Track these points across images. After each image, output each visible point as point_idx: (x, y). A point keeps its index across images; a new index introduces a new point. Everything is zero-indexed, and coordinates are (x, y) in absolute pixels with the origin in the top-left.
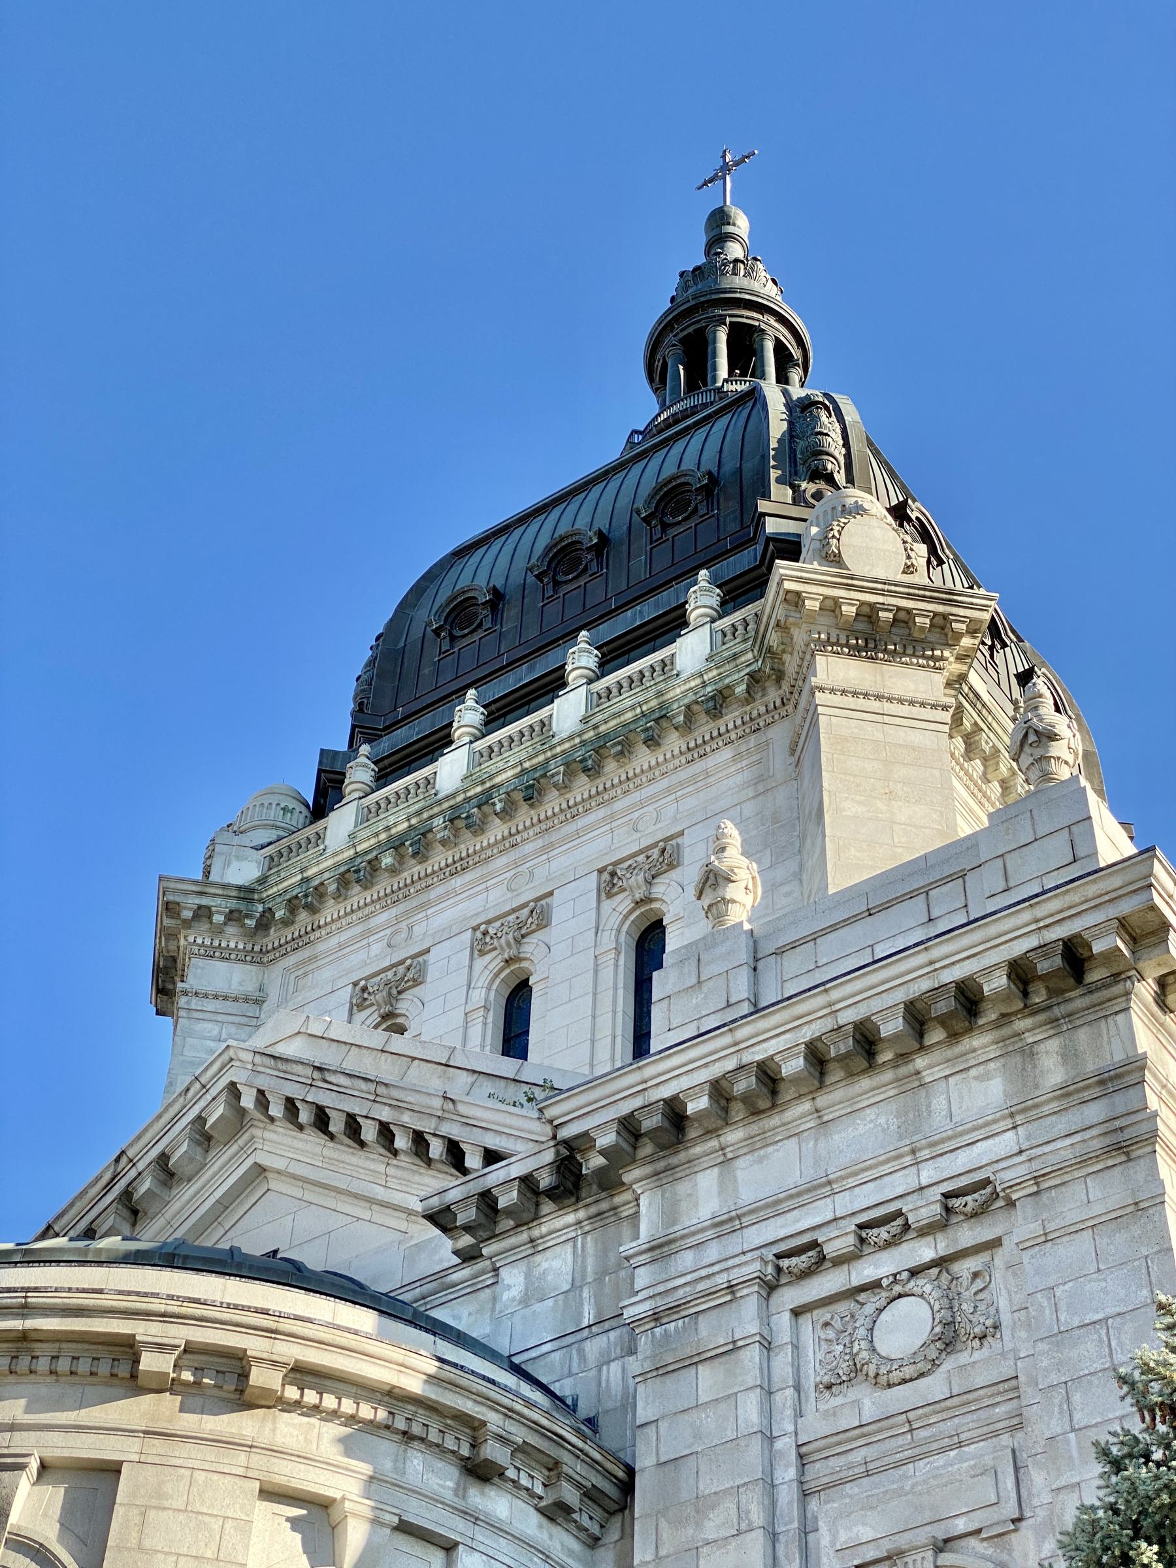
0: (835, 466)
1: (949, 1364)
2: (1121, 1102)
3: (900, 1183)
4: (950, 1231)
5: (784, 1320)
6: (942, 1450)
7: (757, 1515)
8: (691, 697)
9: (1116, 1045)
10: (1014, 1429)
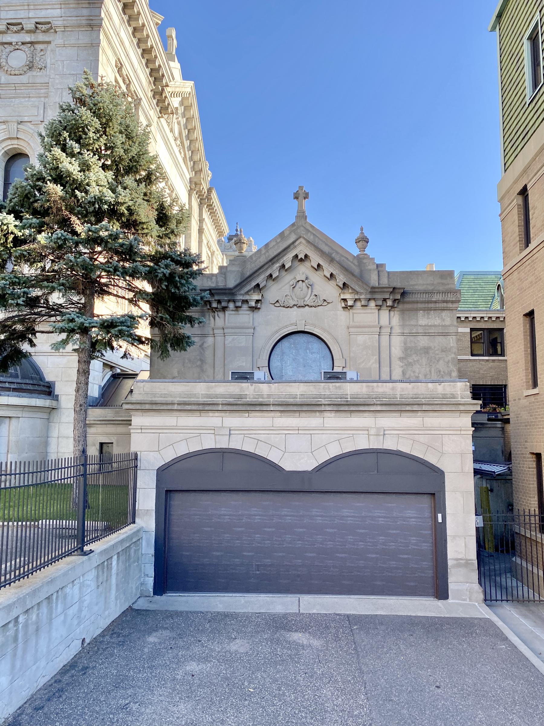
1: (30, 74)
6: (24, 97)
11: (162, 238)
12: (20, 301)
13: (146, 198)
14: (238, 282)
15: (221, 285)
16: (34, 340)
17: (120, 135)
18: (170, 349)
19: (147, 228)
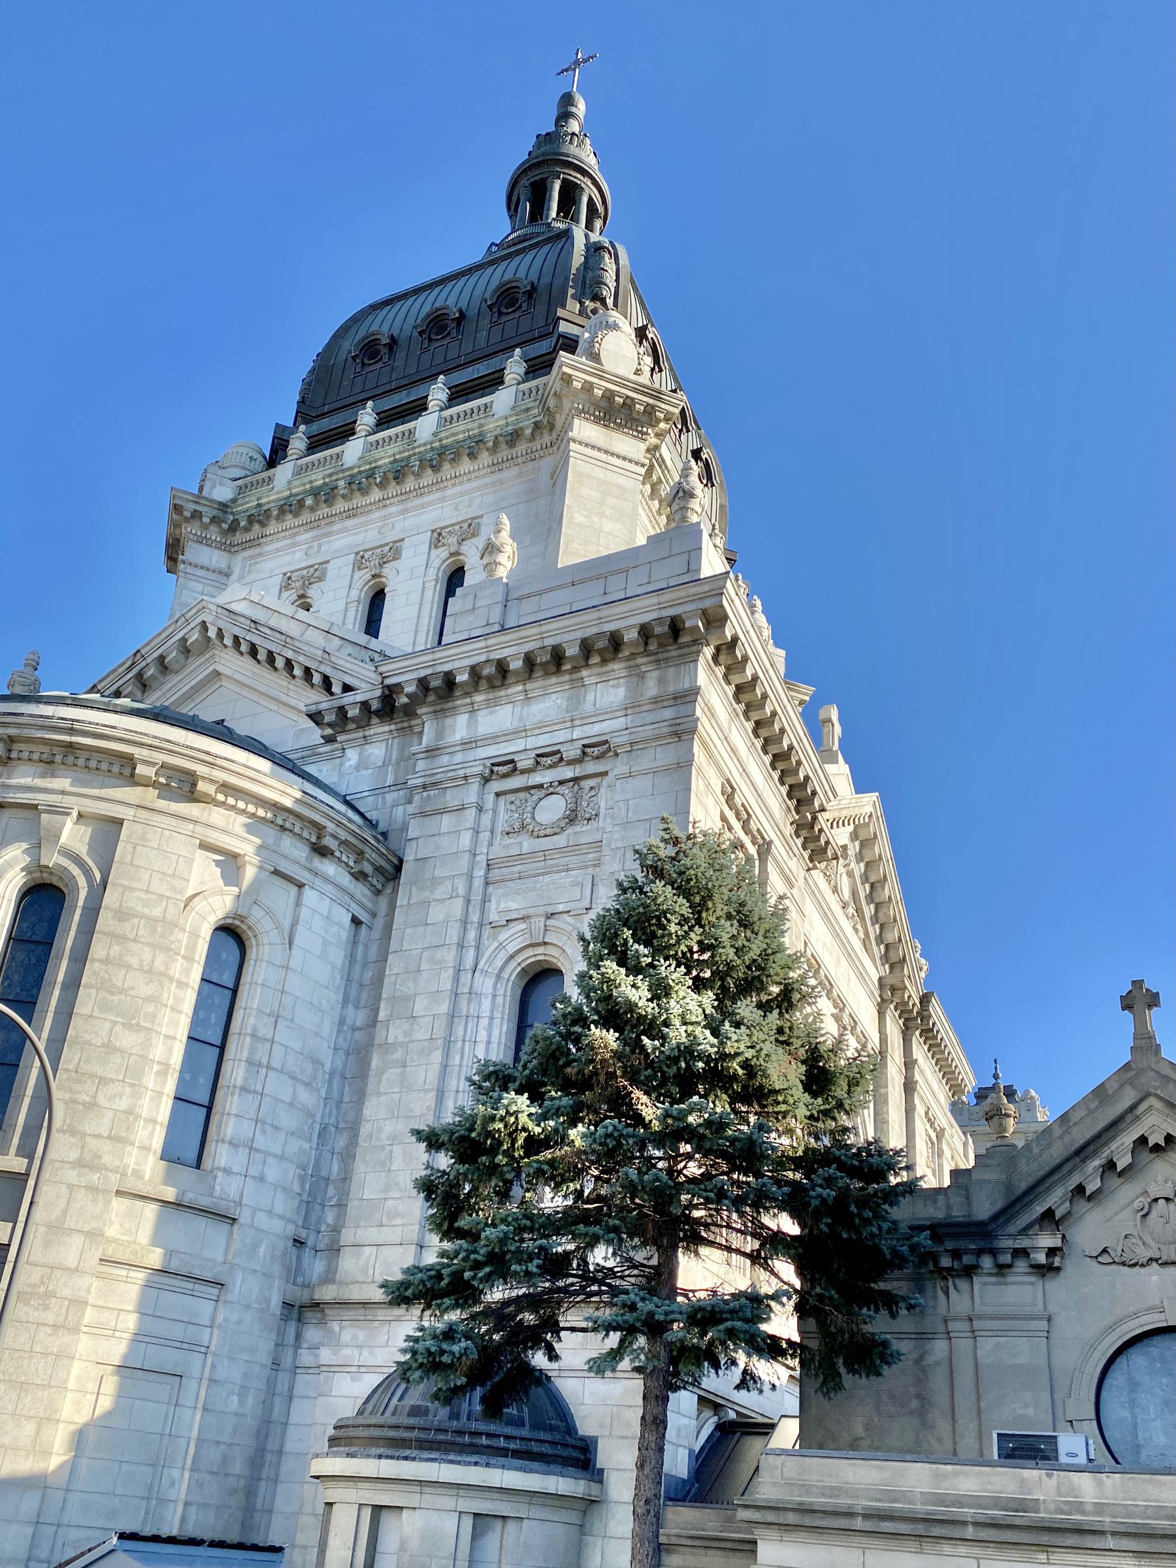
0: (608, 294)
1: (570, 830)
2: (683, 710)
3: (561, 736)
4: (583, 765)
5: (492, 797)
7: (461, 891)
8: (498, 432)
9: (687, 677)
10: (595, 866)
11: (817, 1120)
12: (532, 1267)
13: (781, 1039)
14: (1000, 1204)
15: (958, 1213)
16: (556, 1345)
17: (729, 923)
18: (842, 1370)
19: (785, 1102)
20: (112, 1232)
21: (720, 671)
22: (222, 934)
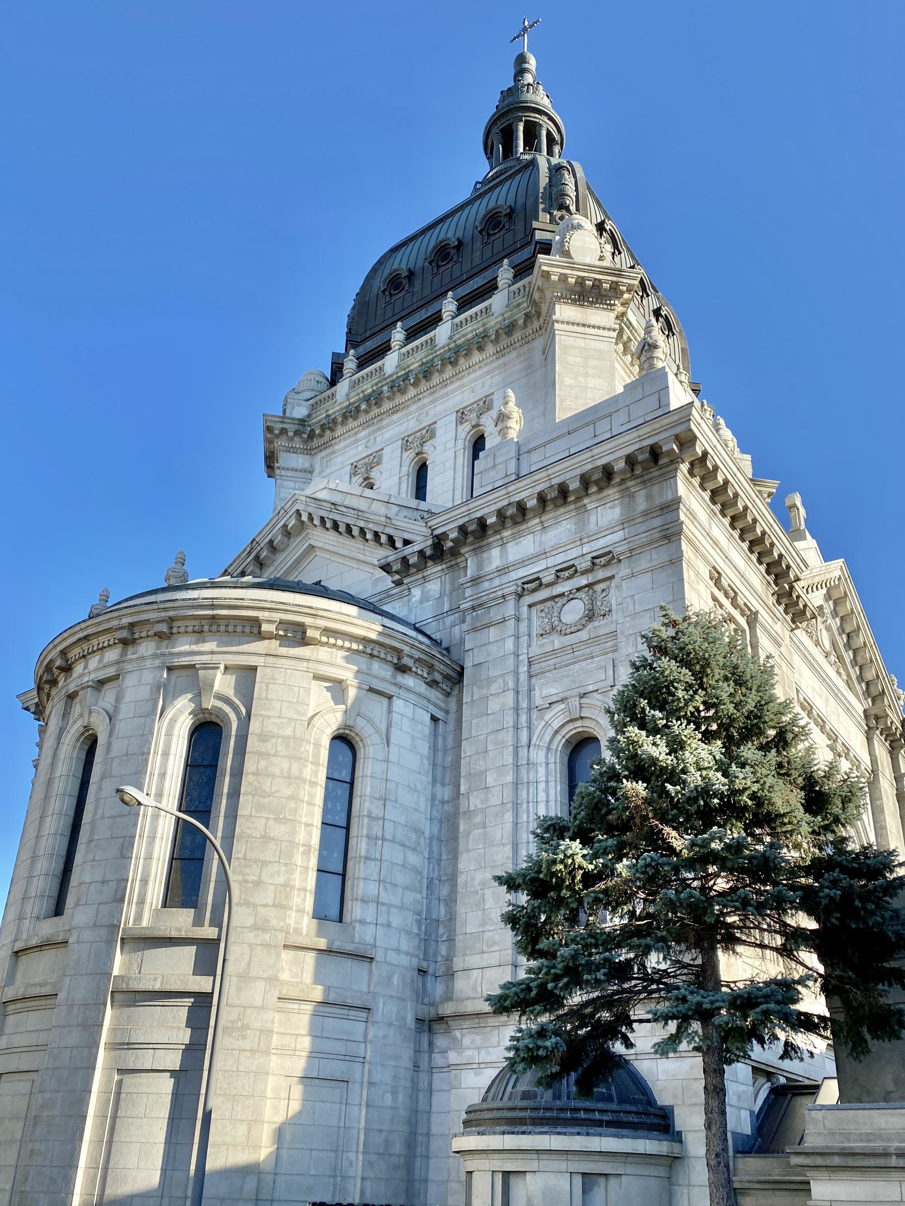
0: (570, 202)
1: (590, 626)
2: (669, 517)
3: (574, 553)
4: (594, 573)
5: (525, 609)
6: (585, 660)
7: (511, 685)
8: (498, 326)
9: (669, 491)
10: (614, 651)
11: (819, 834)
12: (600, 976)
13: (782, 772)
17: (726, 684)
18: (868, 1036)
19: (790, 823)
20: (285, 976)
21: (696, 481)
22: (337, 742)
